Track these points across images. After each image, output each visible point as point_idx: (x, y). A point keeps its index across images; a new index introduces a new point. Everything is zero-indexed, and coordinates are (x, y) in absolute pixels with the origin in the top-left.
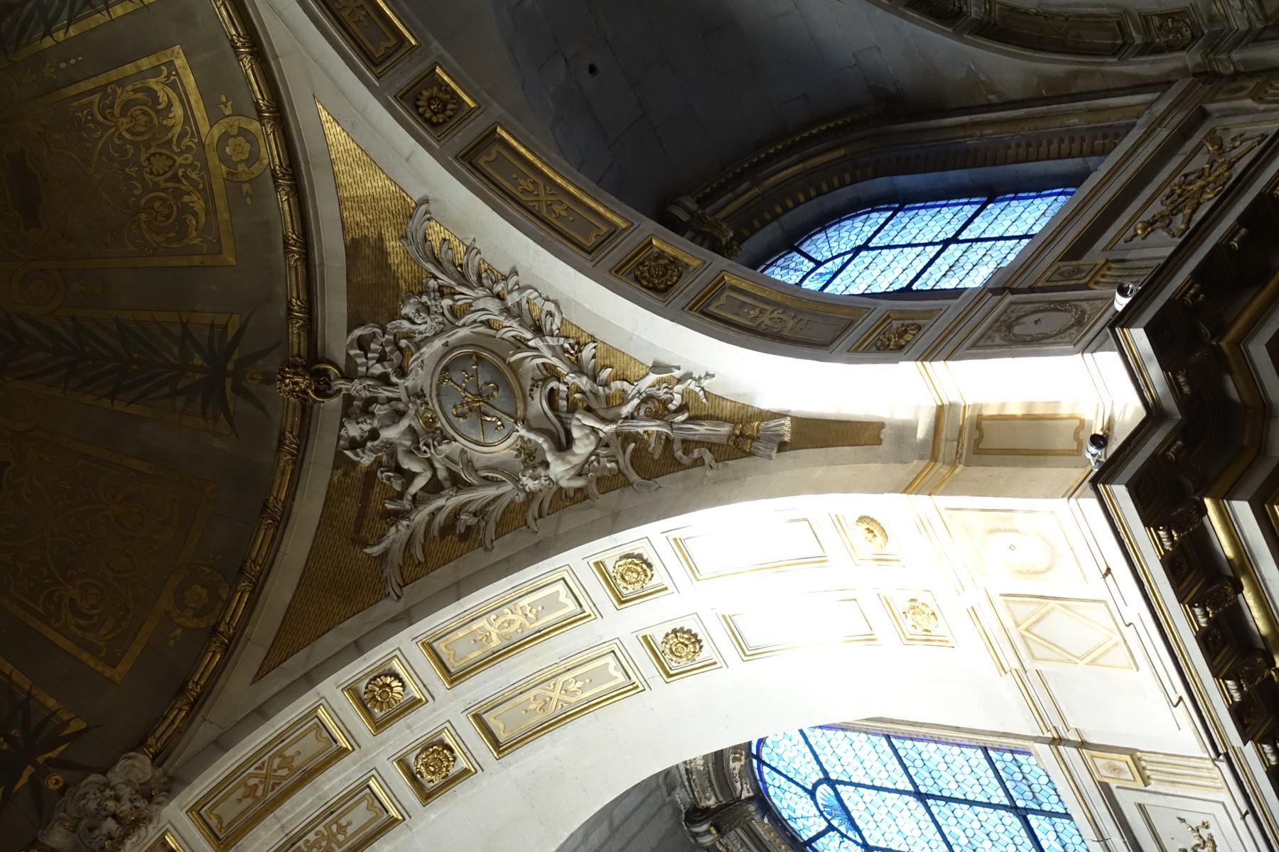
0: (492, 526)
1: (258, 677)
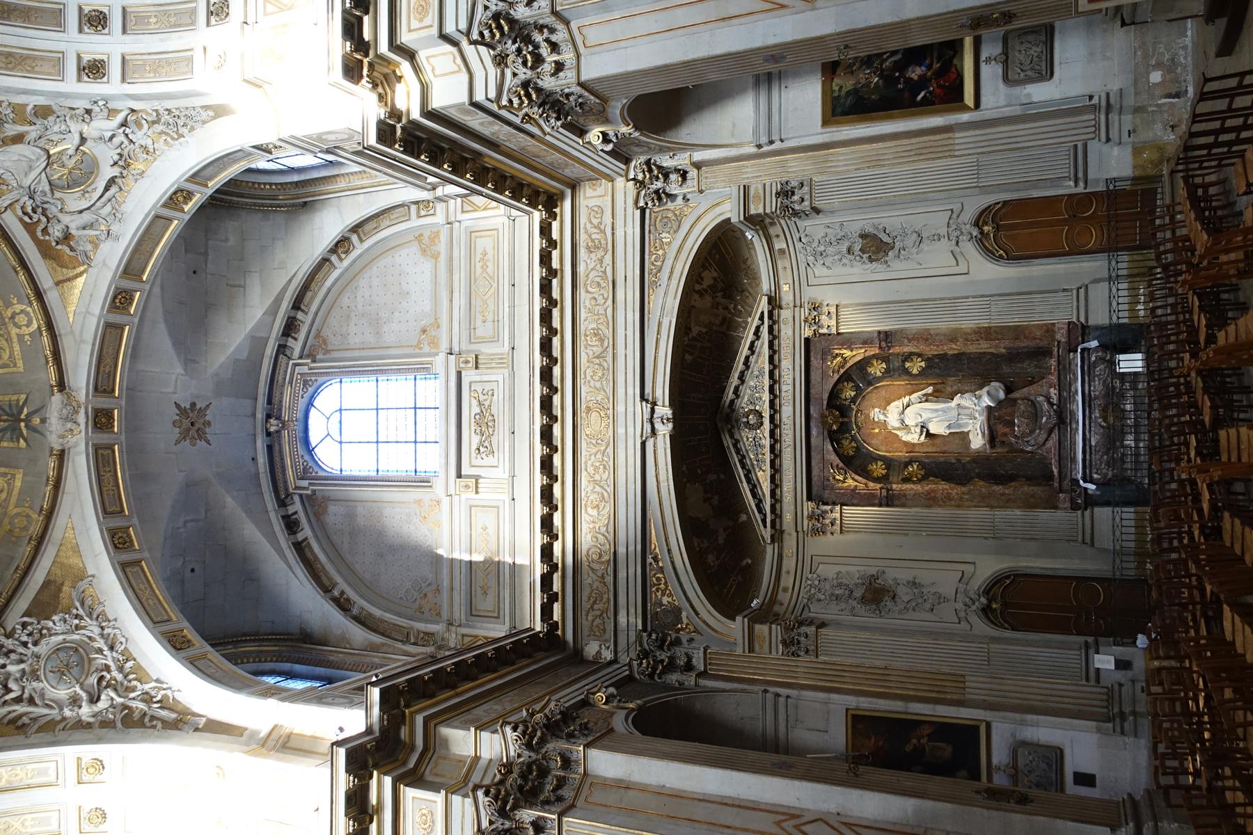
0: (36, 727)
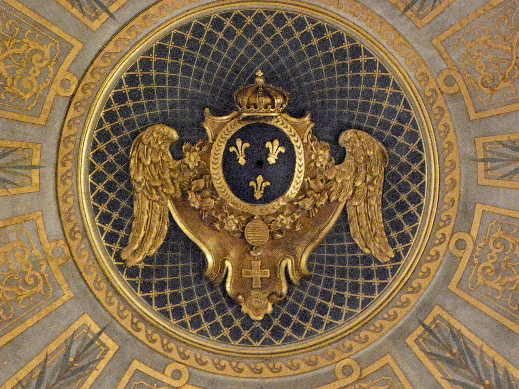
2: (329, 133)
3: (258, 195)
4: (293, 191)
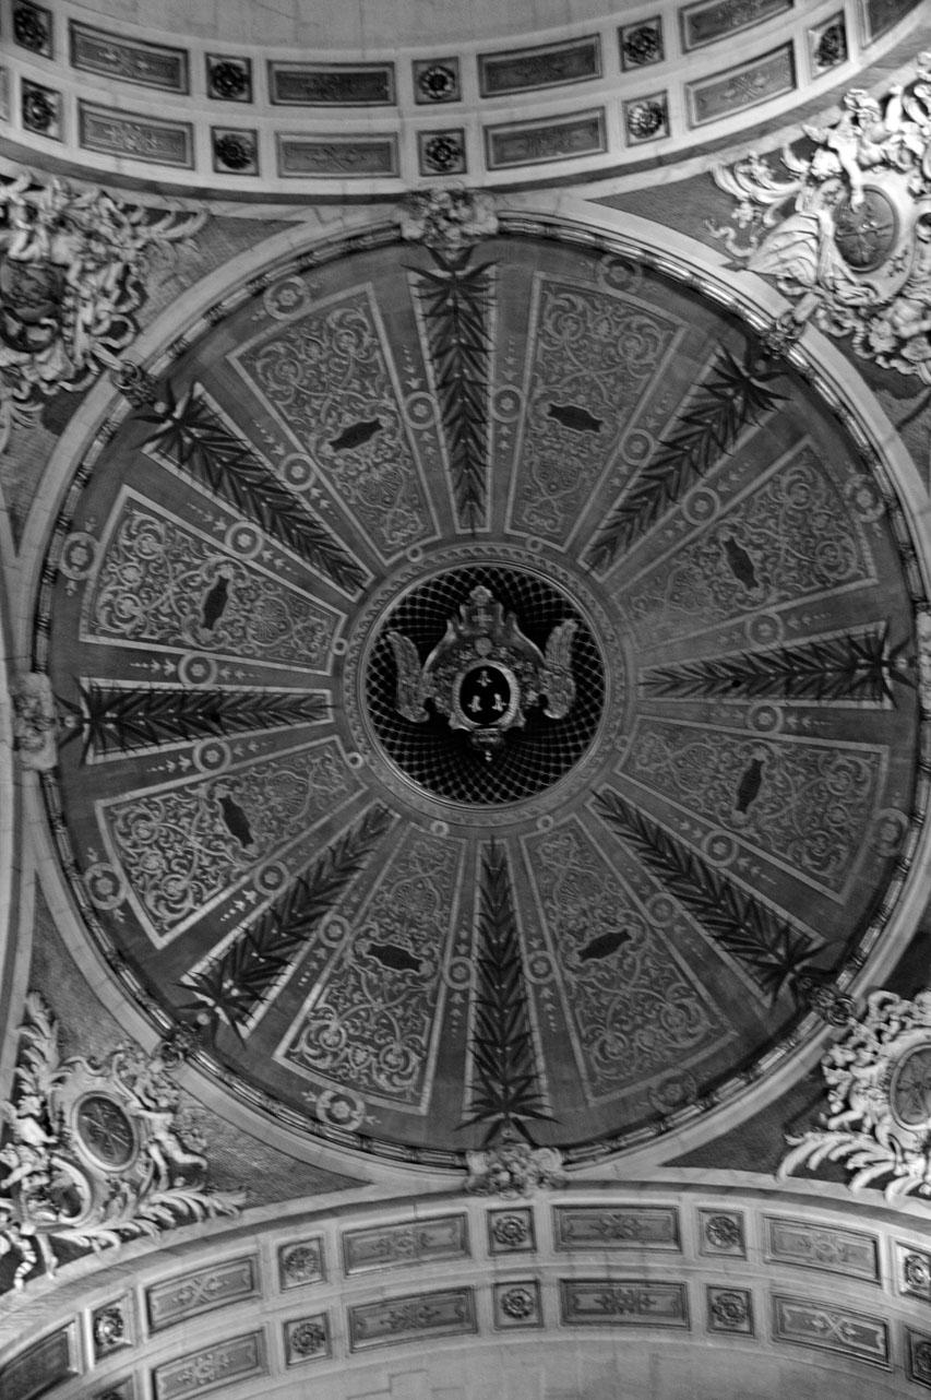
1: (666, 1165)
2: (438, 720)
3: (484, 673)
4: (460, 677)
